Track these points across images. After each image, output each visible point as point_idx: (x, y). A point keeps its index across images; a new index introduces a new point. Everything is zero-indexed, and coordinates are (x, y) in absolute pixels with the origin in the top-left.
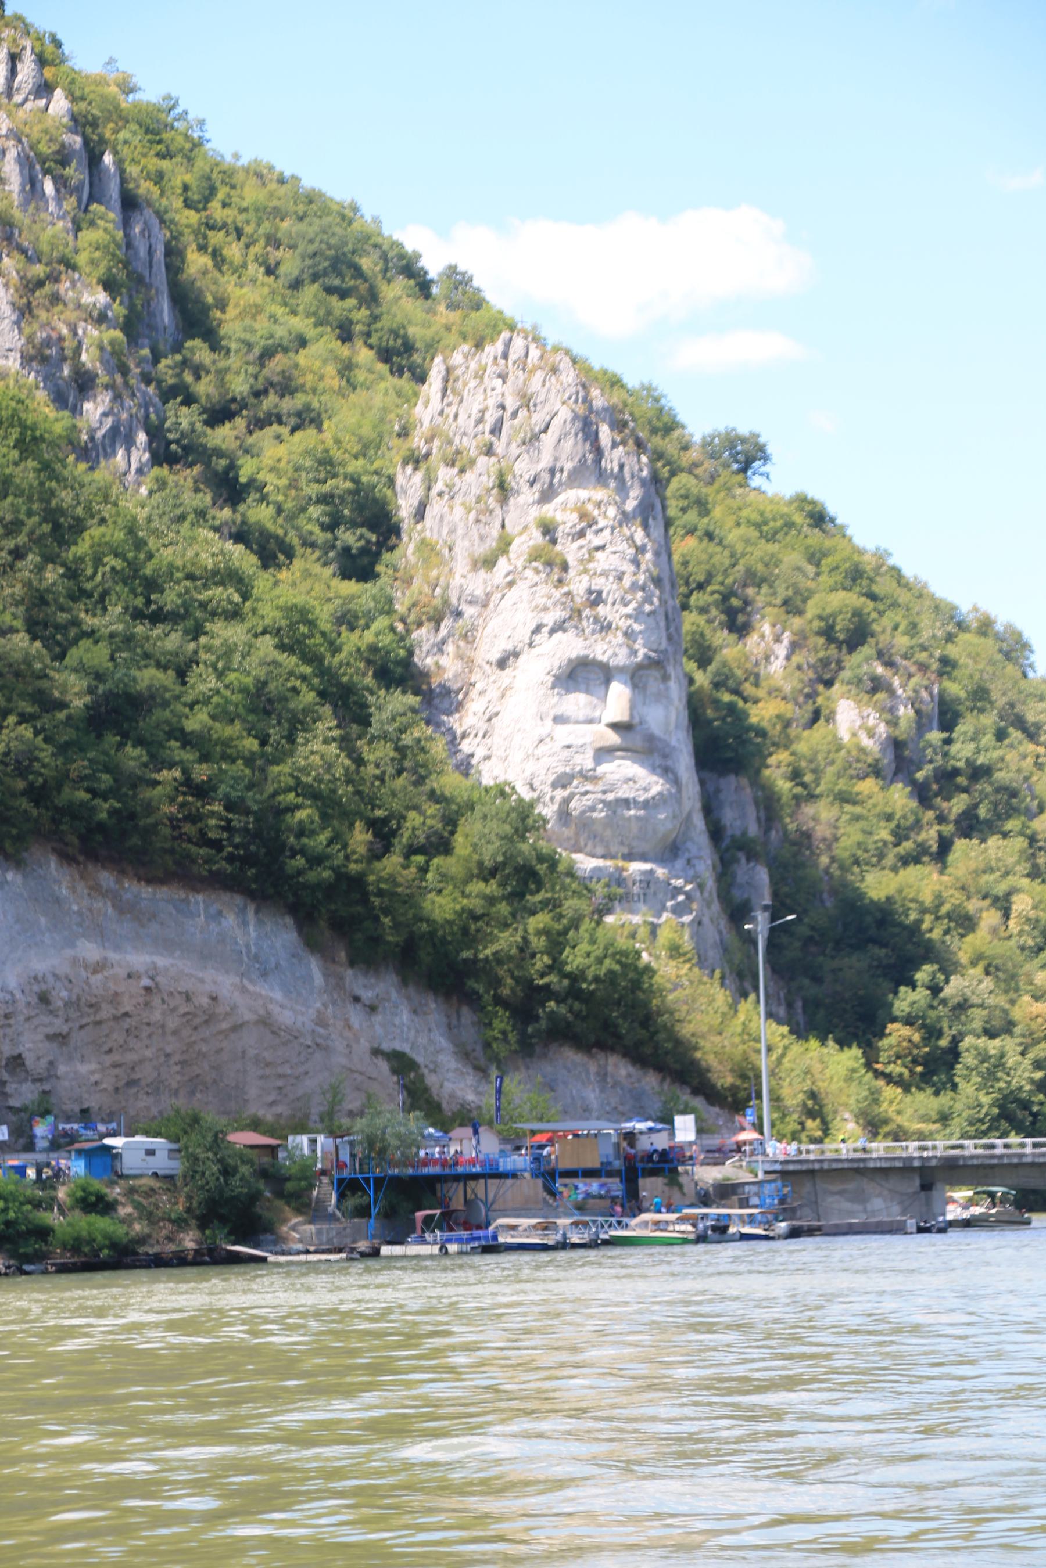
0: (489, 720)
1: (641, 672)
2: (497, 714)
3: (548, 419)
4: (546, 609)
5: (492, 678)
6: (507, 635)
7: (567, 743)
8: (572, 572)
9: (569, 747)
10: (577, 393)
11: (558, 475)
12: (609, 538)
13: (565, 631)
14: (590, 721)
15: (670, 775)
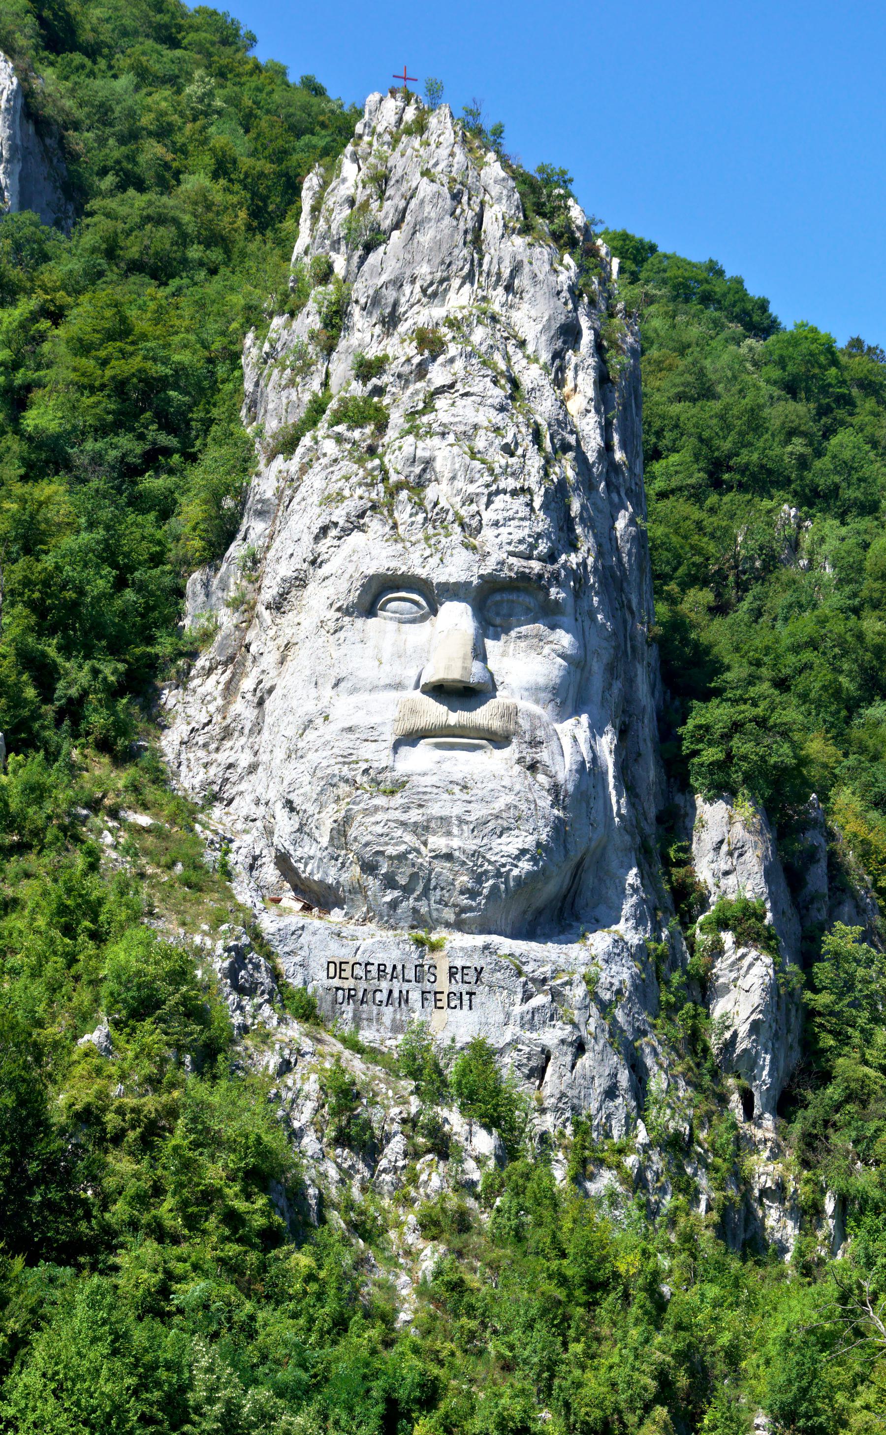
0: (261, 703)
1: (498, 597)
2: (270, 691)
3: (402, 204)
4: (340, 497)
5: (271, 633)
6: (290, 552)
7: (347, 725)
8: (391, 434)
9: (350, 729)
10: (452, 155)
11: (407, 288)
12: (462, 373)
13: (362, 528)
14: (398, 686)
15: (541, 778)
